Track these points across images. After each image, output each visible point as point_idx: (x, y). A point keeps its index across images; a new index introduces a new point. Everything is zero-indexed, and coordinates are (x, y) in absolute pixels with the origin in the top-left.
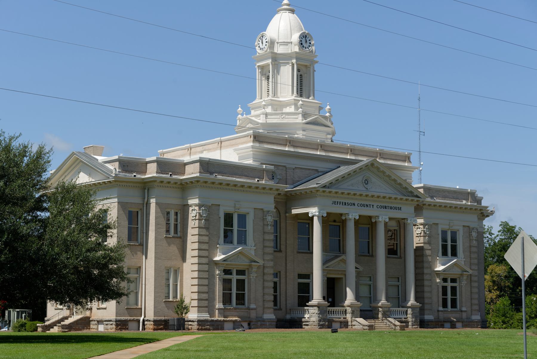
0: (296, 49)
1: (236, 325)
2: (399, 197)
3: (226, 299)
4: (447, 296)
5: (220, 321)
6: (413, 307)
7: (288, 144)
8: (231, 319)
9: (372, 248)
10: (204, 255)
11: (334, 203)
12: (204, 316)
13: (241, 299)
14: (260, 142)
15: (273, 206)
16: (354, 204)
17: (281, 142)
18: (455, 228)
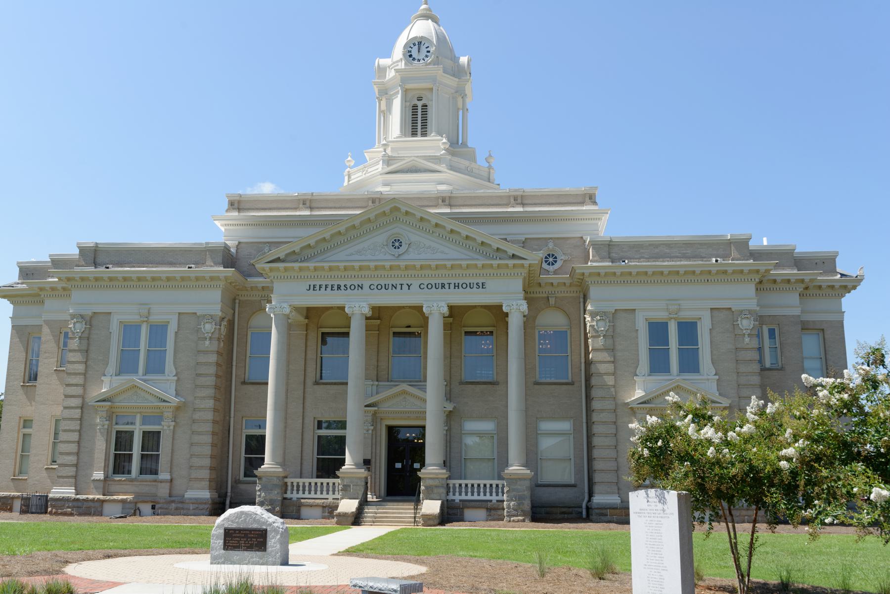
0: (402, 65)
1: (132, 510)
3: (120, 464)
5: (93, 500)
6: (513, 480)
7: (301, 206)
8: (115, 497)
10: (74, 394)
12: (63, 493)
13: (150, 465)
14: (239, 210)
15: (219, 307)
17: (287, 206)
18: (687, 315)
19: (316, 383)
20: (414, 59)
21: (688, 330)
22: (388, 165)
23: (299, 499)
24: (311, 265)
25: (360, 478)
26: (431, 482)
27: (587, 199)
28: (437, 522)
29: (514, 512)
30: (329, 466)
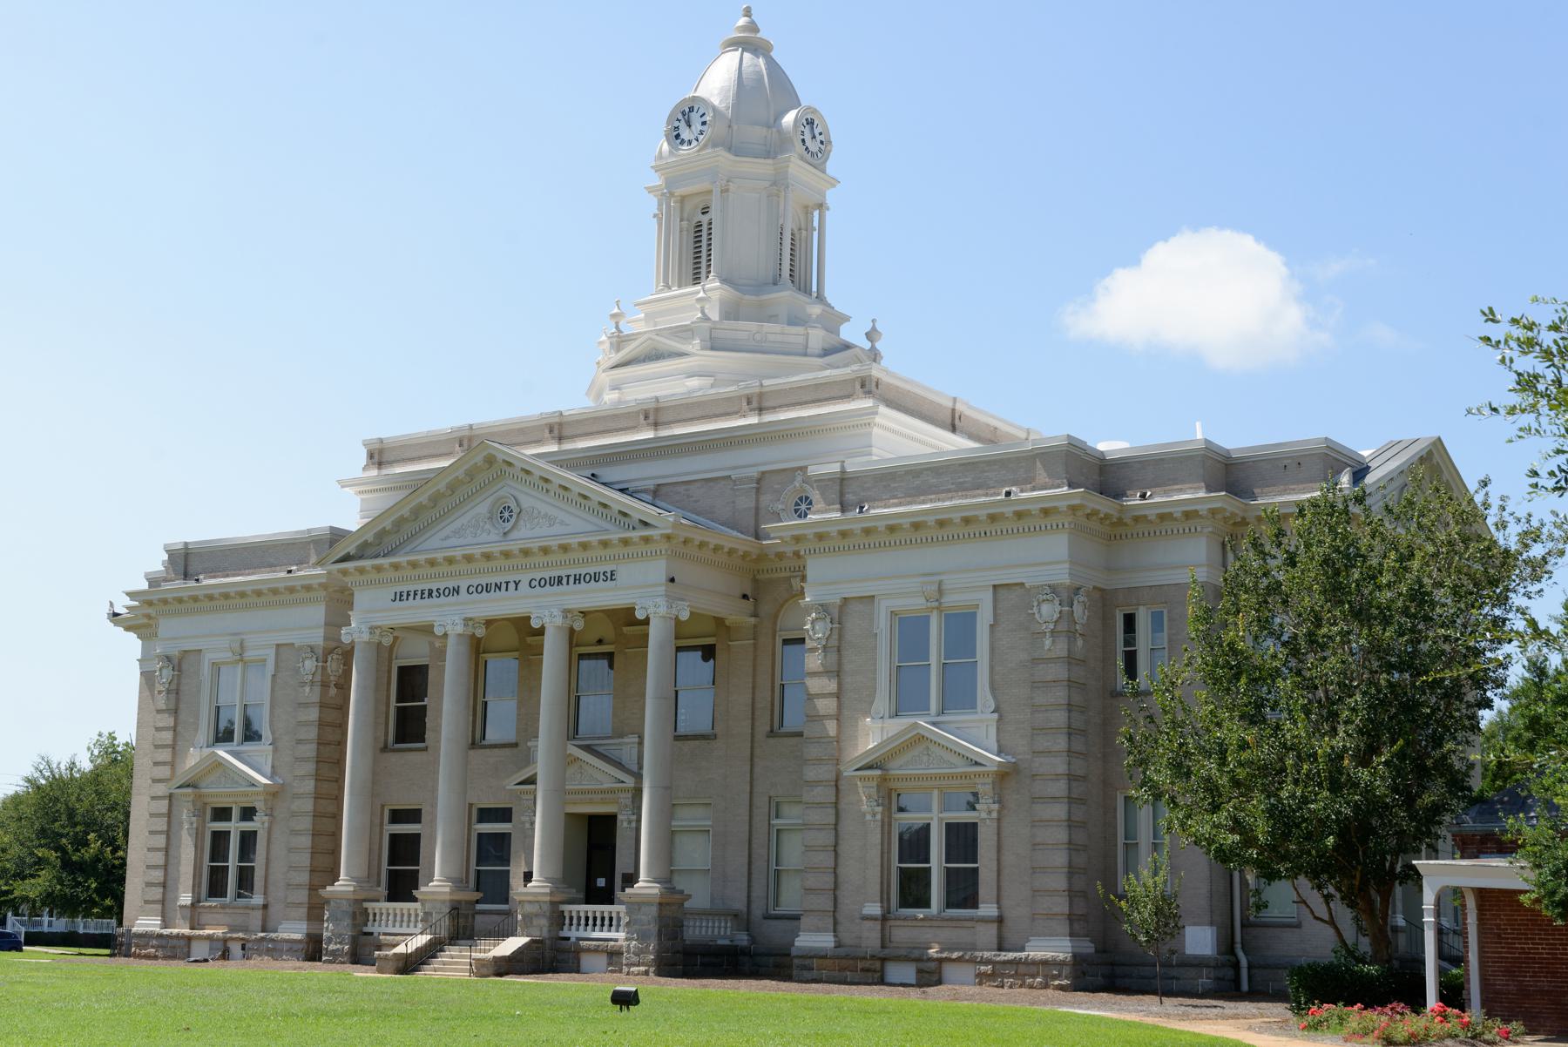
2: (615, 535)
4: (927, 860)
5: (178, 936)
9: (773, 705)
11: (399, 597)
15: (321, 632)
16: (457, 591)
19: (772, 733)
20: (682, 142)
21: (961, 626)
22: (618, 350)
23: (579, 939)
24: (400, 559)
25: (443, 902)
26: (529, 909)
27: (858, 386)
28: (491, 971)
29: (635, 959)
30: (402, 886)
